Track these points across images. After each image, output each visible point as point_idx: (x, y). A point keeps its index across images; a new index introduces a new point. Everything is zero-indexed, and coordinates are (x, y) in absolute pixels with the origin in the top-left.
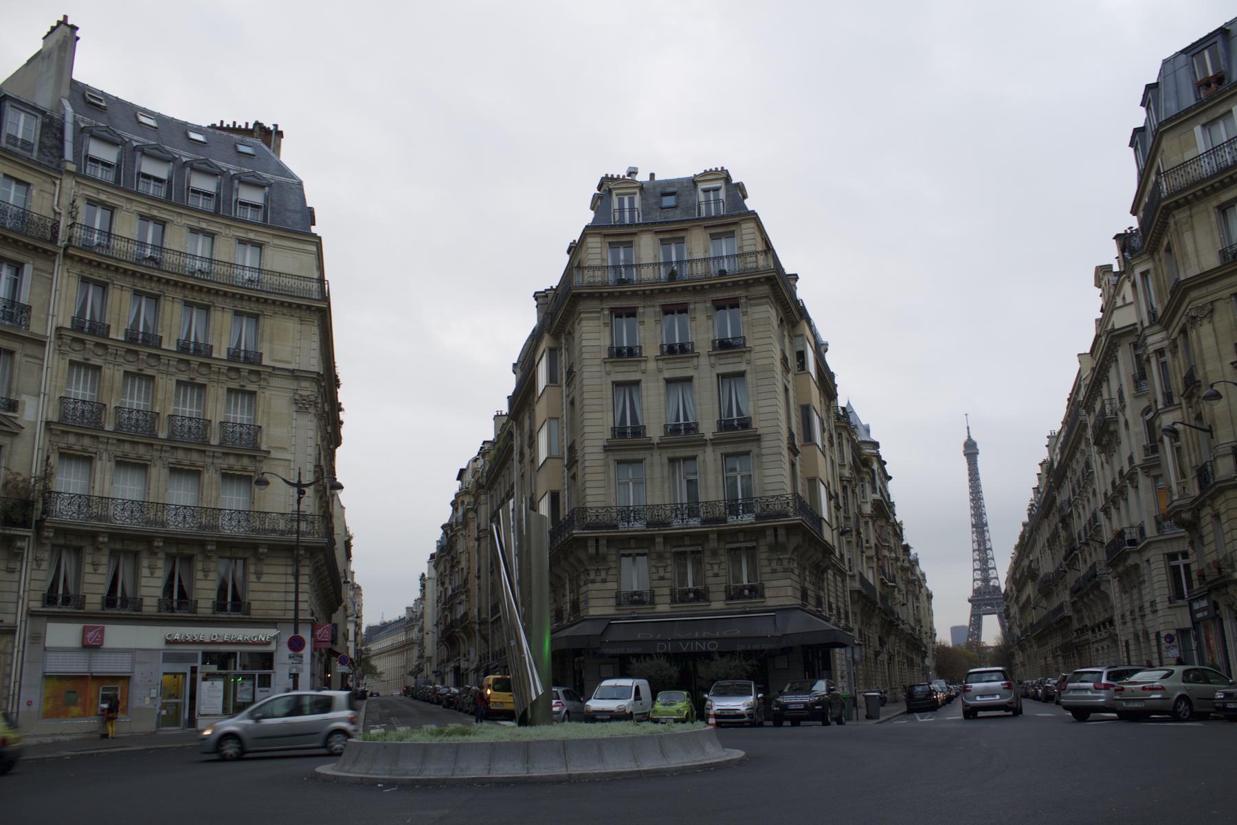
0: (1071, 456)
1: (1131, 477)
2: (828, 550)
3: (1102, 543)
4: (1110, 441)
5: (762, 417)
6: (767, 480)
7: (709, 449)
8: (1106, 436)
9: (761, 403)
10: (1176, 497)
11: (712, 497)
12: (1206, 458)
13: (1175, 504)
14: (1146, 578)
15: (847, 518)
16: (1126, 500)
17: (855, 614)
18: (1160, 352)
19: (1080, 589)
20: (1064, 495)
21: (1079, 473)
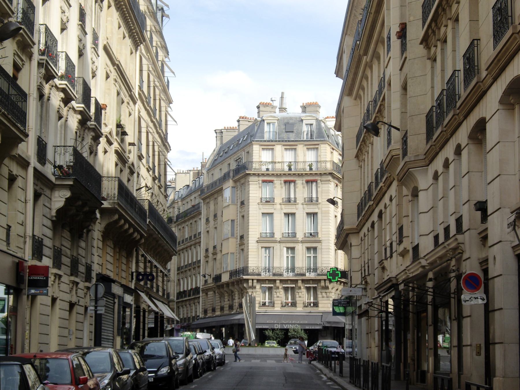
11: (300, 266)
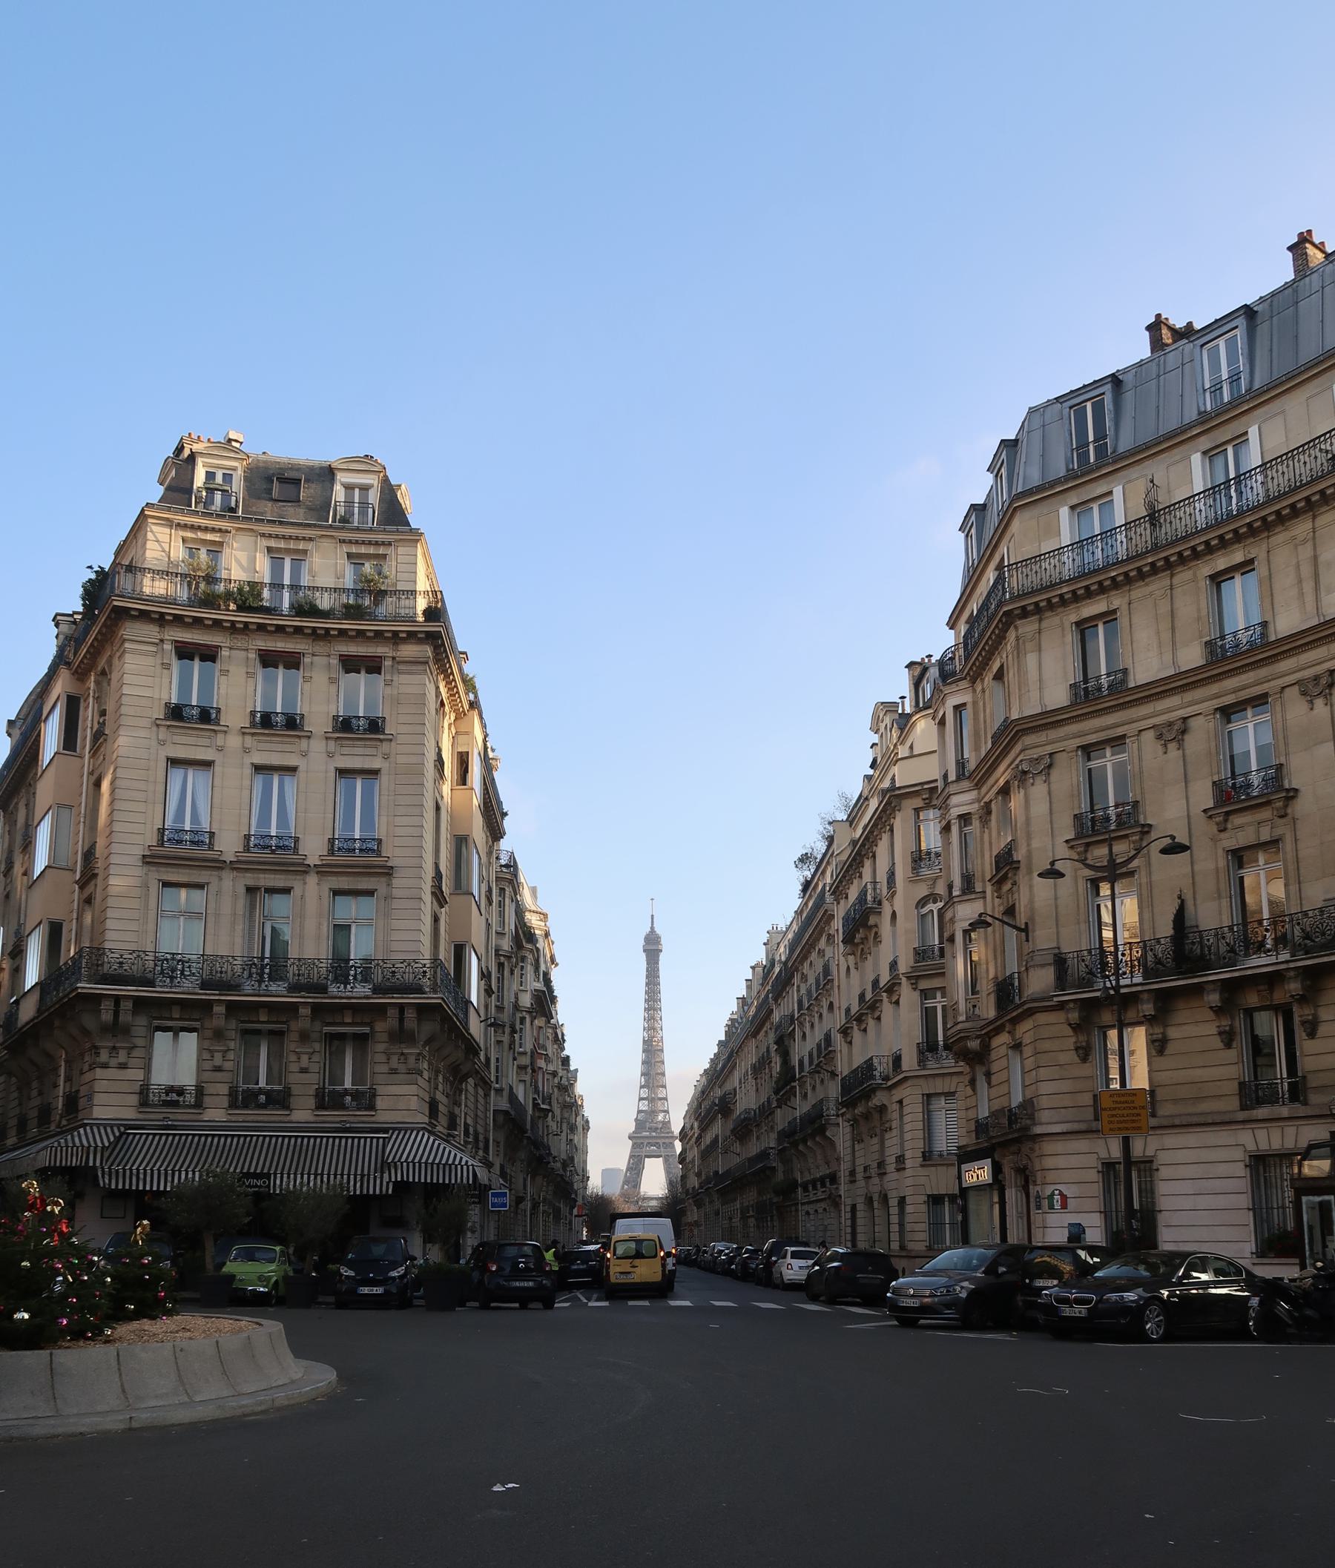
0: (804, 956)
1: (892, 988)
2: (471, 1048)
3: (833, 1075)
4: (865, 939)
5: (398, 842)
6: (395, 936)
7: (312, 879)
8: (861, 928)
9: (399, 821)
10: (962, 1018)
11: (309, 953)
12: (1013, 967)
13: (959, 1027)
14: (894, 1124)
15: (500, 1009)
16: (879, 1019)
17: (497, 1143)
18: (965, 819)
19: (793, 1133)
20: (789, 1005)
21: (811, 980)
